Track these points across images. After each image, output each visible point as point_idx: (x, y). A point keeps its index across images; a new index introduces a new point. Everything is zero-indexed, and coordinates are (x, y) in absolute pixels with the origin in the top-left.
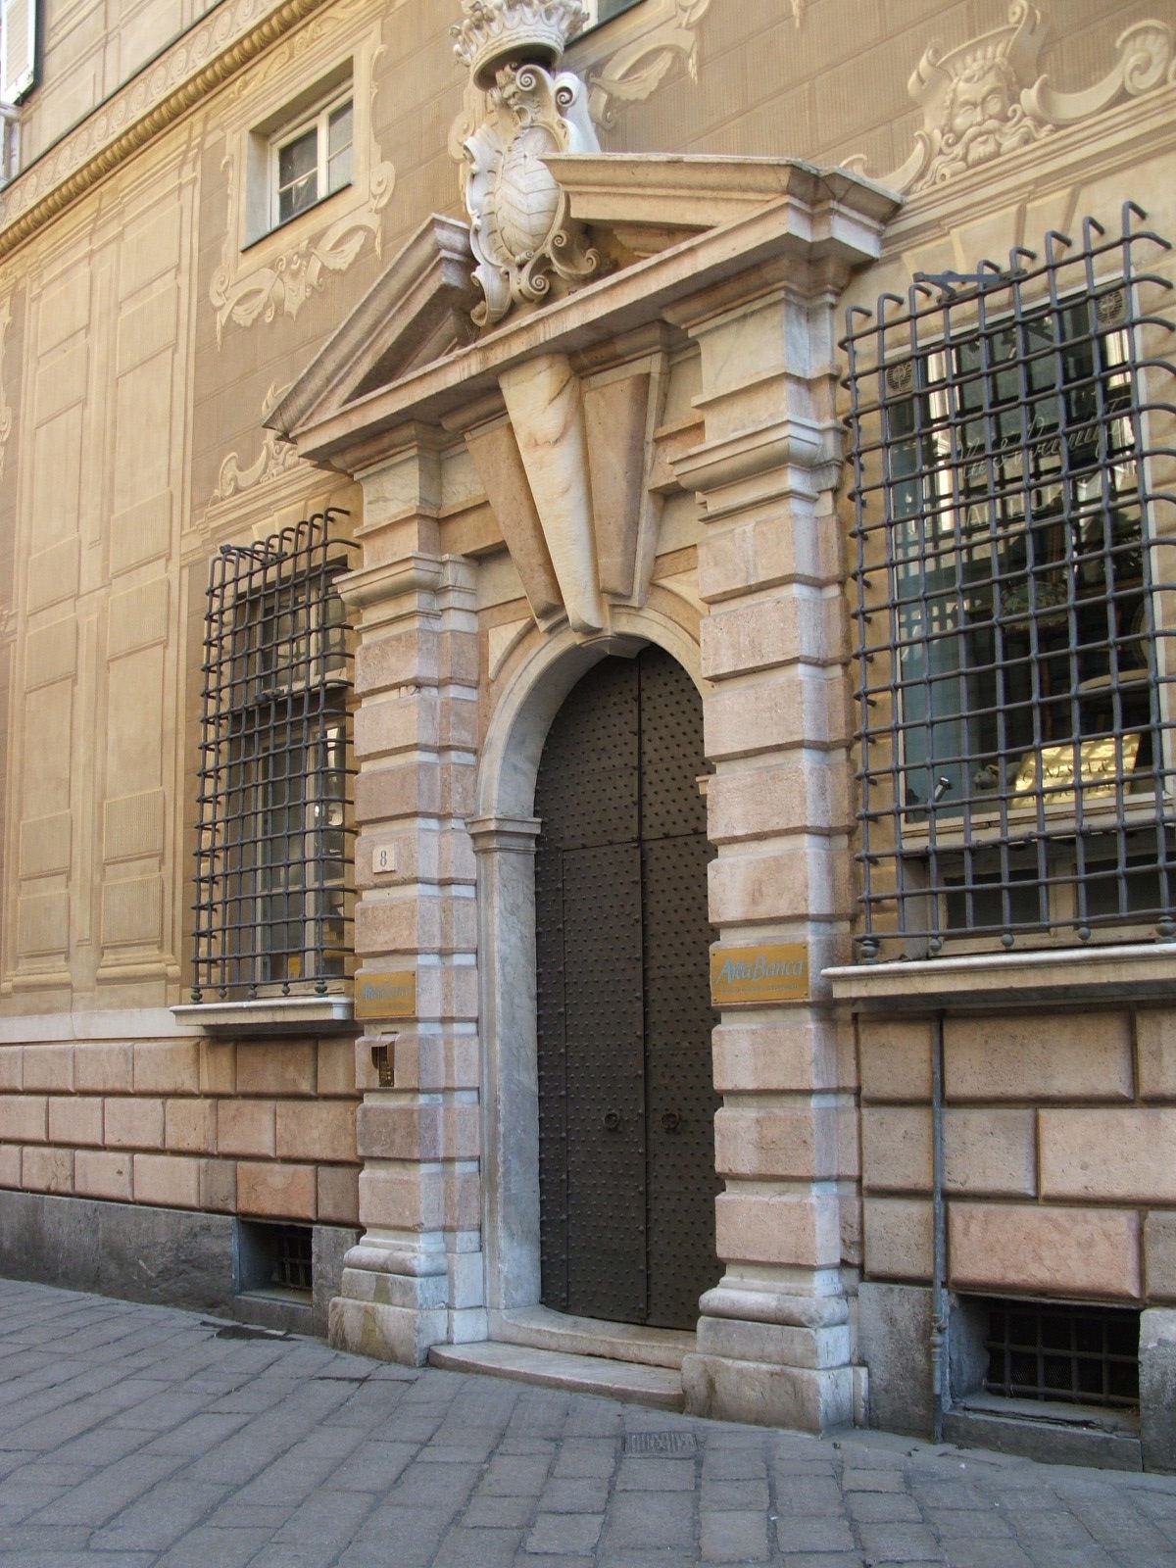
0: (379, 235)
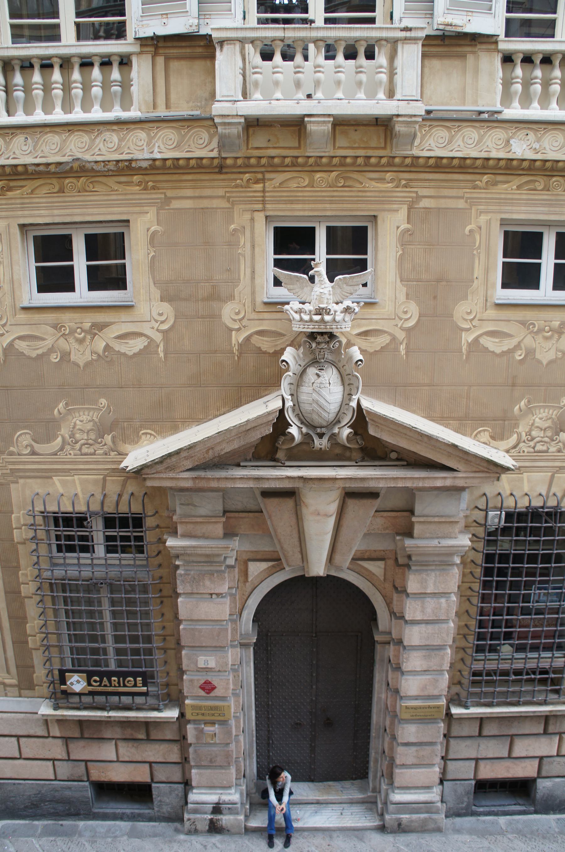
0: (162, 345)
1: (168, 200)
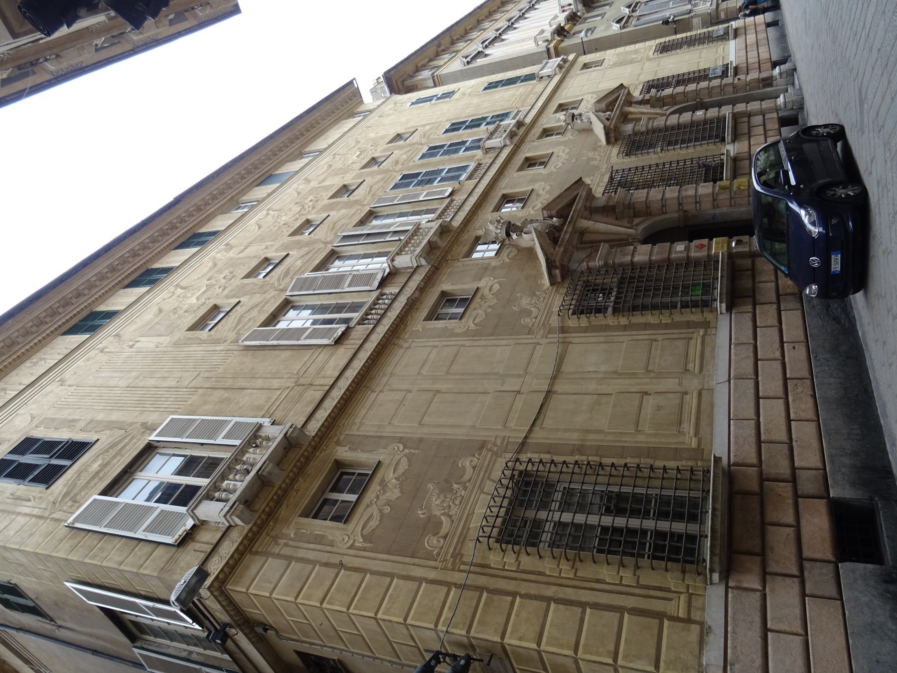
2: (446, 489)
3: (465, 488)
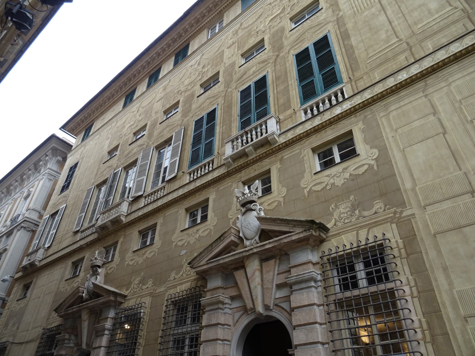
1: (218, 188)
2: (353, 210)
3: (357, 219)
